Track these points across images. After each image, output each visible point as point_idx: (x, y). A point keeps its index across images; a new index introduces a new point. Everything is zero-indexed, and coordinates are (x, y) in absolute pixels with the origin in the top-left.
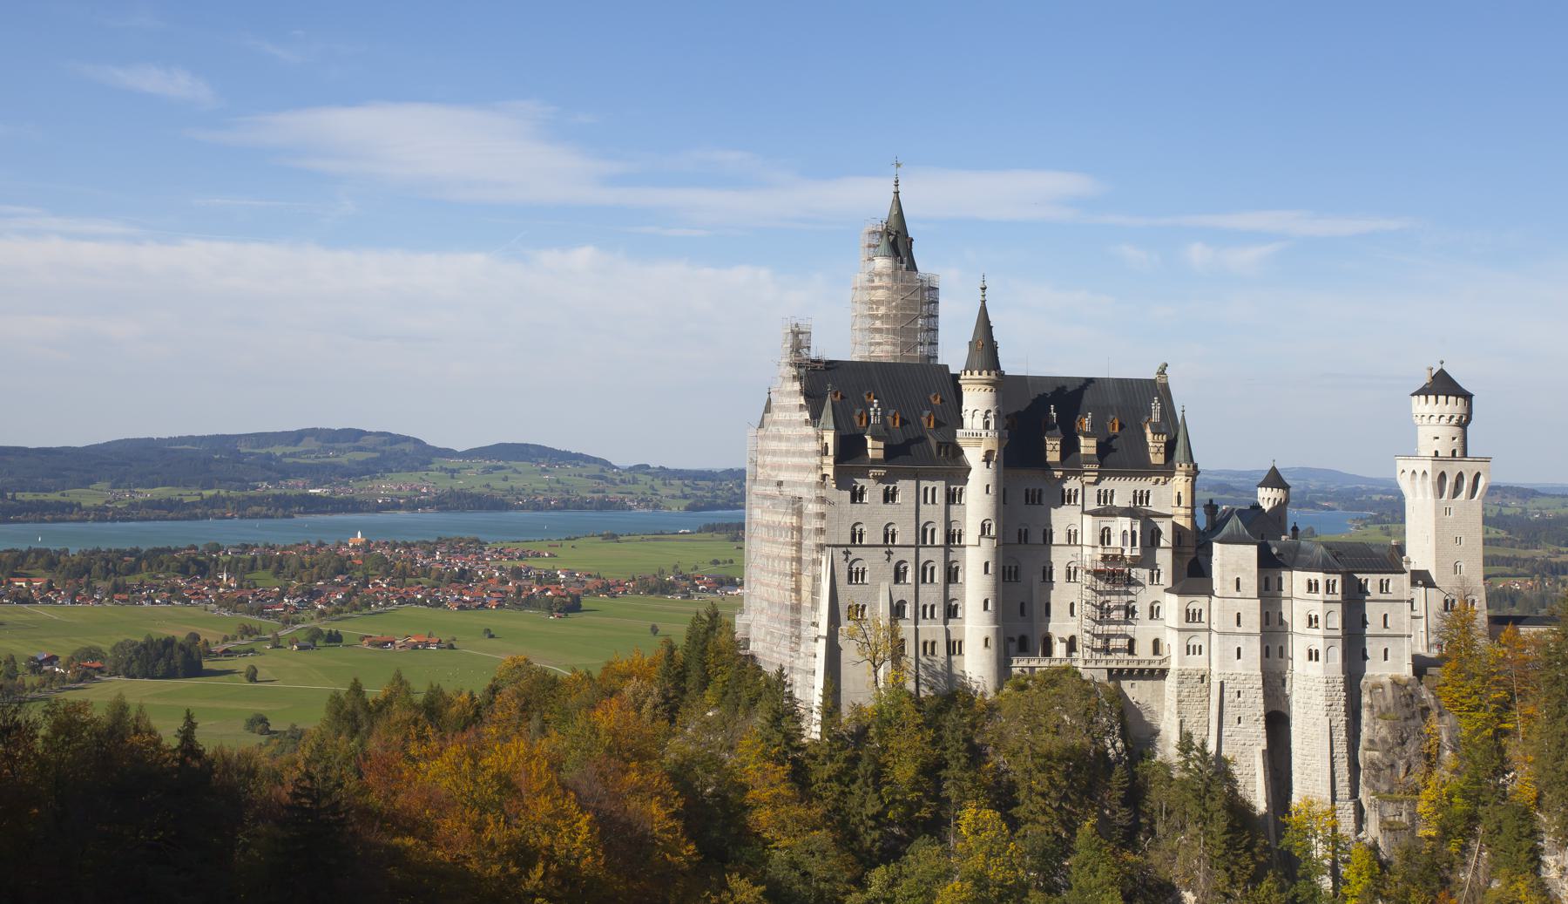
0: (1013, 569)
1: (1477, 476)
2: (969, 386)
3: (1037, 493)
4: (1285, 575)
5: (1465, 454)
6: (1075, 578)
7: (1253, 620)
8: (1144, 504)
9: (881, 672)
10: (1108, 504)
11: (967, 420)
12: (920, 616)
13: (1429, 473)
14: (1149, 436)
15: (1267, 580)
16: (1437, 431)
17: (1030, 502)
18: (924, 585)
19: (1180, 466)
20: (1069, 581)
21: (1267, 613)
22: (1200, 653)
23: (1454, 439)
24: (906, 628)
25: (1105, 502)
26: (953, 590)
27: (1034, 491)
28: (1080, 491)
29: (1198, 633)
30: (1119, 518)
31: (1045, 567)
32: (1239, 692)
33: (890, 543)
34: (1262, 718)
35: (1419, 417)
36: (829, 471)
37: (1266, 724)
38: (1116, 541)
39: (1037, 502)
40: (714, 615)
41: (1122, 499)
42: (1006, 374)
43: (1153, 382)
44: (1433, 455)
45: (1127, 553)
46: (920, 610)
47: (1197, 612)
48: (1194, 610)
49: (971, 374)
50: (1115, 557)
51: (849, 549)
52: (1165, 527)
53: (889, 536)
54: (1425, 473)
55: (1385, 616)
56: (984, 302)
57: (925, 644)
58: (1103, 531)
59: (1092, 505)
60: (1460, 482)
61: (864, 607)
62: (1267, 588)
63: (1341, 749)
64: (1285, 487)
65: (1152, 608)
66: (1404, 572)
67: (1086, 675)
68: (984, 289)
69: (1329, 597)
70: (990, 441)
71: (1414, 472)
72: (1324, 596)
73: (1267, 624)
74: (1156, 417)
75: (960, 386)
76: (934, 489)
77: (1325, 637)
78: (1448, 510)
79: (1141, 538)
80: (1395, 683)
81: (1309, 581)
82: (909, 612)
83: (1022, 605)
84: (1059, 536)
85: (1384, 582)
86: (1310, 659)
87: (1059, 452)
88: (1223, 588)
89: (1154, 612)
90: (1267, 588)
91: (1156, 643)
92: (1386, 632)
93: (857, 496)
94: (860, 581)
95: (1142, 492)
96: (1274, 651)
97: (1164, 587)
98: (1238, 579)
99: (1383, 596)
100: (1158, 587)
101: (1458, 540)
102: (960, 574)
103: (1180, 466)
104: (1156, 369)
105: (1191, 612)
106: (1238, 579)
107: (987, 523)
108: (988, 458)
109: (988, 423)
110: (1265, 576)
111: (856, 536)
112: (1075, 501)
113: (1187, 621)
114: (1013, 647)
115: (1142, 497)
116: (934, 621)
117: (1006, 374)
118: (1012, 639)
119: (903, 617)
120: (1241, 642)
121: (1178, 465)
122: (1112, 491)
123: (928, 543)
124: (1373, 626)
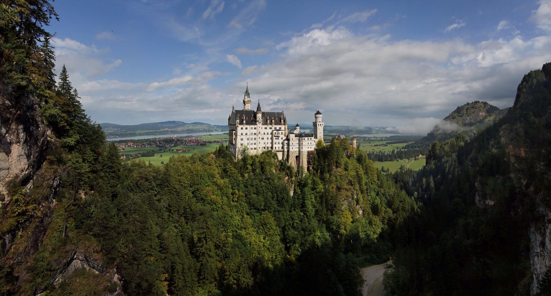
4: (298, 138)
24: (248, 147)
41: (278, 129)
50: (276, 136)
53: (246, 134)
67: (273, 152)
74: (282, 117)
80: (312, 151)
93: (242, 129)
111: (242, 134)
115: (280, 128)
120: (293, 147)
124: (310, 144)
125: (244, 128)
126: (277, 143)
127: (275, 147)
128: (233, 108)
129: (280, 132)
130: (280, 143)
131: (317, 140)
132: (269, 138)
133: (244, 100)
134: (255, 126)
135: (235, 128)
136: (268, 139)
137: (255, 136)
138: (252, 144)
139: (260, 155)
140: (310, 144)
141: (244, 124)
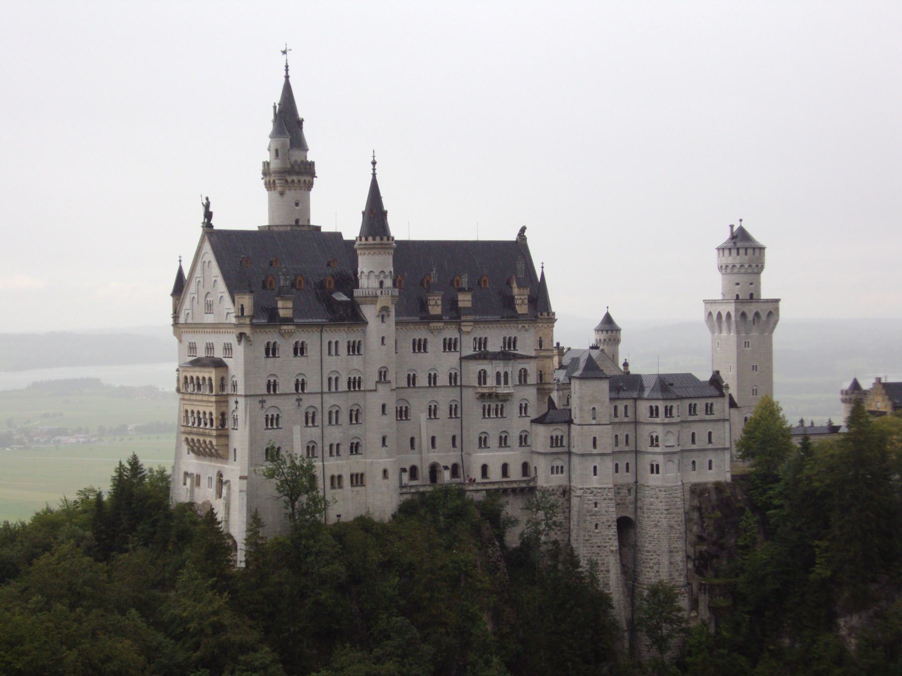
0: (404, 409)
1: (770, 314)
2: (363, 252)
3: (422, 343)
4: (630, 403)
5: (759, 294)
6: (455, 414)
7: (606, 444)
8: (512, 349)
9: (297, 503)
10: (483, 349)
11: (363, 282)
12: (327, 454)
13: (733, 314)
14: (516, 291)
15: (616, 408)
16: (737, 278)
17: (417, 351)
18: (330, 427)
19: (541, 315)
20: (451, 418)
21: (616, 436)
22: (562, 472)
23: (751, 284)
25: (480, 348)
26: (355, 431)
27: (420, 340)
28: (459, 340)
29: (561, 457)
30: (494, 362)
31: (430, 406)
32: (596, 504)
33: (300, 391)
34: (616, 523)
35: (724, 267)
36: (247, 331)
37: (618, 529)
38: (491, 381)
39: (422, 351)
40: (135, 464)
41: (495, 346)
42: (396, 239)
43: (516, 242)
44: (735, 298)
45: (500, 391)
46: (327, 449)
47: (559, 438)
48: (557, 437)
49: (366, 240)
51: (264, 398)
52: (532, 368)
53: (300, 385)
54: (729, 315)
55: (710, 433)
56: (374, 175)
57: (332, 478)
58: (480, 373)
59: (469, 351)
60: (755, 321)
61: (279, 449)
62: (616, 415)
63: (680, 545)
64: (618, 330)
65: (521, 437)
66: (722, 395)
68: (374, 163)
69: (667, 420)
70: (384, 300)
71: (719, 315)
72: (663, 420)
73: (617, 445)
75: (355, 251)
76: (337, 343)
77: (664, 454)
78: (747, 343)
79: (512, 377)
80: (719, 487)
81: (651, 407)
82: (318, 452)
83: (412, 439)
84: (443, 380)
85: (709, 405)
86: (652, 472)
87: (440, 307)
88: (582, 417)
89: (523, 440)
90: (616, 415)
91: (525, 466)
92: (710, 446)
93: (271, 351)
94: (275, 426)
95: (510, 338)
96: (622, 467)
97: (531, 419)
98: (594, 409)
99: (708, 417)
100: (528, 418)
101: (754, 368)
102: (360, 416)
103: (541, 315)
104: (517, 231)
105: (554, 438)
106: (594, 409)
107: (383, 370)
108: (383, 314)
109: (381, 283)
110: (614, 405)
111: (272, 387)
112: (455, 348)
113: (552, 446)
114: (406, 477)
115: (511, 343)
116: (339, 457)
117: (396, 239)
118: (404, 470)
119: (313, 455)
120: (597, 461)
121: (539, 314)
122: (486, 339)
123: (333, 389)
124: (701, 442)
125: (286, 347)
126: (493, 442)
127: (484, 468)
128: (208, 215)
129: (513, 369)
130: (514, 440)
131: (737, 419)
132: (443, 412)
133: (266, 165)
134: (354, 337)
135: (228, 348)
136: (433, 412)
137: (355, 398)
138: (334, 450)
139: (387, 517)
140: (701, 442)
141: (287, 321)
